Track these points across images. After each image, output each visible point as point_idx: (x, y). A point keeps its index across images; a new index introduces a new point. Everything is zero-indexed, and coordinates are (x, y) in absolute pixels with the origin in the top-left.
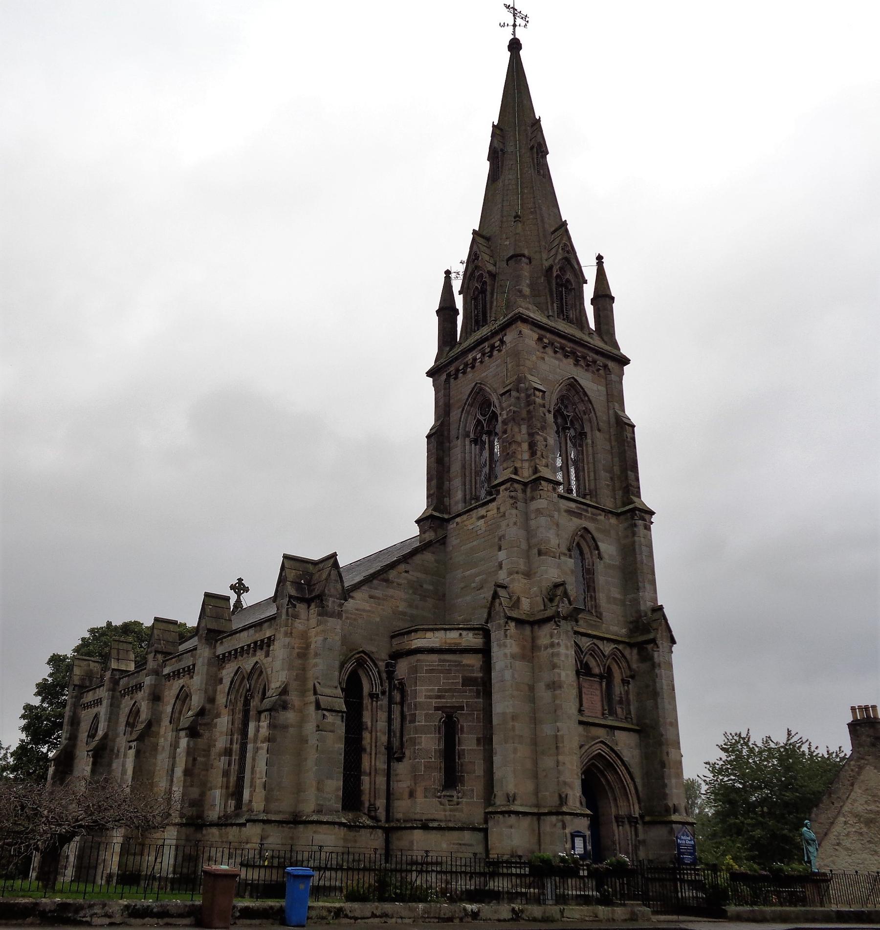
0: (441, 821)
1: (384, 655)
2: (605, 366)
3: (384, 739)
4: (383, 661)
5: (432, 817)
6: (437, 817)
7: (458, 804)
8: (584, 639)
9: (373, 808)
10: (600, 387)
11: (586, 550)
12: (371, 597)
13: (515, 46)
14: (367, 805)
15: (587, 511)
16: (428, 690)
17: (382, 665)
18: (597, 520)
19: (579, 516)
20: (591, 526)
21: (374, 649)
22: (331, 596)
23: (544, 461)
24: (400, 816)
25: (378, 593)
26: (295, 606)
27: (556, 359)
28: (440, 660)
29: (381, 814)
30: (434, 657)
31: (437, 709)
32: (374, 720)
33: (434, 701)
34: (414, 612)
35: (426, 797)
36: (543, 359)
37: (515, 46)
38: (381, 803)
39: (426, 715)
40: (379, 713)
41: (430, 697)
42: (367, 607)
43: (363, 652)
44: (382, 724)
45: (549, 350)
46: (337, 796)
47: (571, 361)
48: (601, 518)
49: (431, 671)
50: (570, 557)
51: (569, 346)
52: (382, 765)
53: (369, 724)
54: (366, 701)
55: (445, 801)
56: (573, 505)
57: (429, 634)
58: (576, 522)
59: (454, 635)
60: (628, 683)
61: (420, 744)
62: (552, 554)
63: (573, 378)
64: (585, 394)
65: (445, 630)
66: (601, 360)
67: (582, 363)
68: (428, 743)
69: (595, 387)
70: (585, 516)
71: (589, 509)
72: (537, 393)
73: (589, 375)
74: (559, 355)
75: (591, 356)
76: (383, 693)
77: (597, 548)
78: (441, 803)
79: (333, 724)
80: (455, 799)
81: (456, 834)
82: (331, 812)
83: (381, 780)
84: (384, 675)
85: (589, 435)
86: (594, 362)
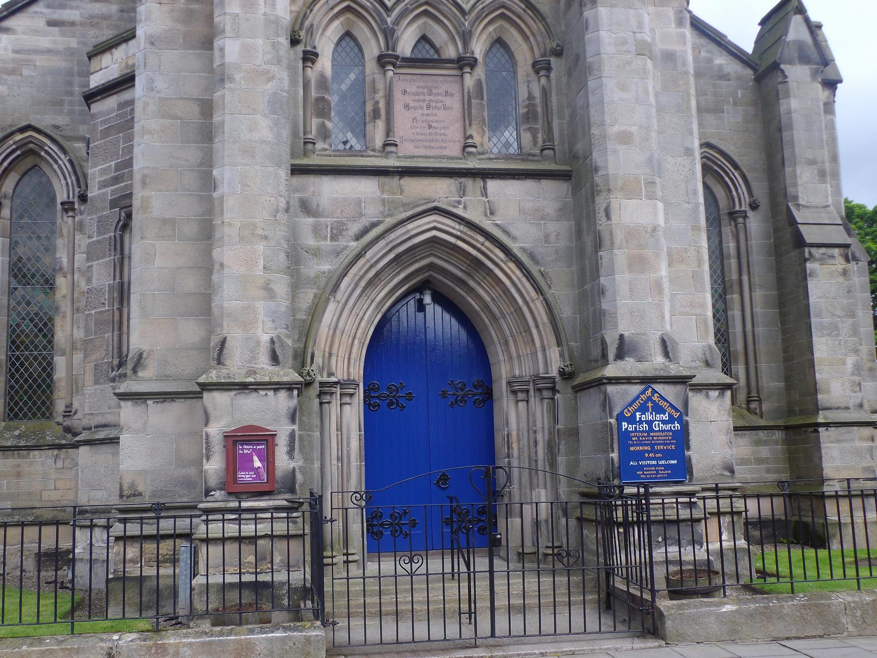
12: (51, 23)
14: (60, 407)
16: (104, 172)
33: (109, 189)
35: (96, 382)
42: (44, 42)
43: (29, 127)
49: (106, 133)
53: (65, 261)
60: (549, 69)
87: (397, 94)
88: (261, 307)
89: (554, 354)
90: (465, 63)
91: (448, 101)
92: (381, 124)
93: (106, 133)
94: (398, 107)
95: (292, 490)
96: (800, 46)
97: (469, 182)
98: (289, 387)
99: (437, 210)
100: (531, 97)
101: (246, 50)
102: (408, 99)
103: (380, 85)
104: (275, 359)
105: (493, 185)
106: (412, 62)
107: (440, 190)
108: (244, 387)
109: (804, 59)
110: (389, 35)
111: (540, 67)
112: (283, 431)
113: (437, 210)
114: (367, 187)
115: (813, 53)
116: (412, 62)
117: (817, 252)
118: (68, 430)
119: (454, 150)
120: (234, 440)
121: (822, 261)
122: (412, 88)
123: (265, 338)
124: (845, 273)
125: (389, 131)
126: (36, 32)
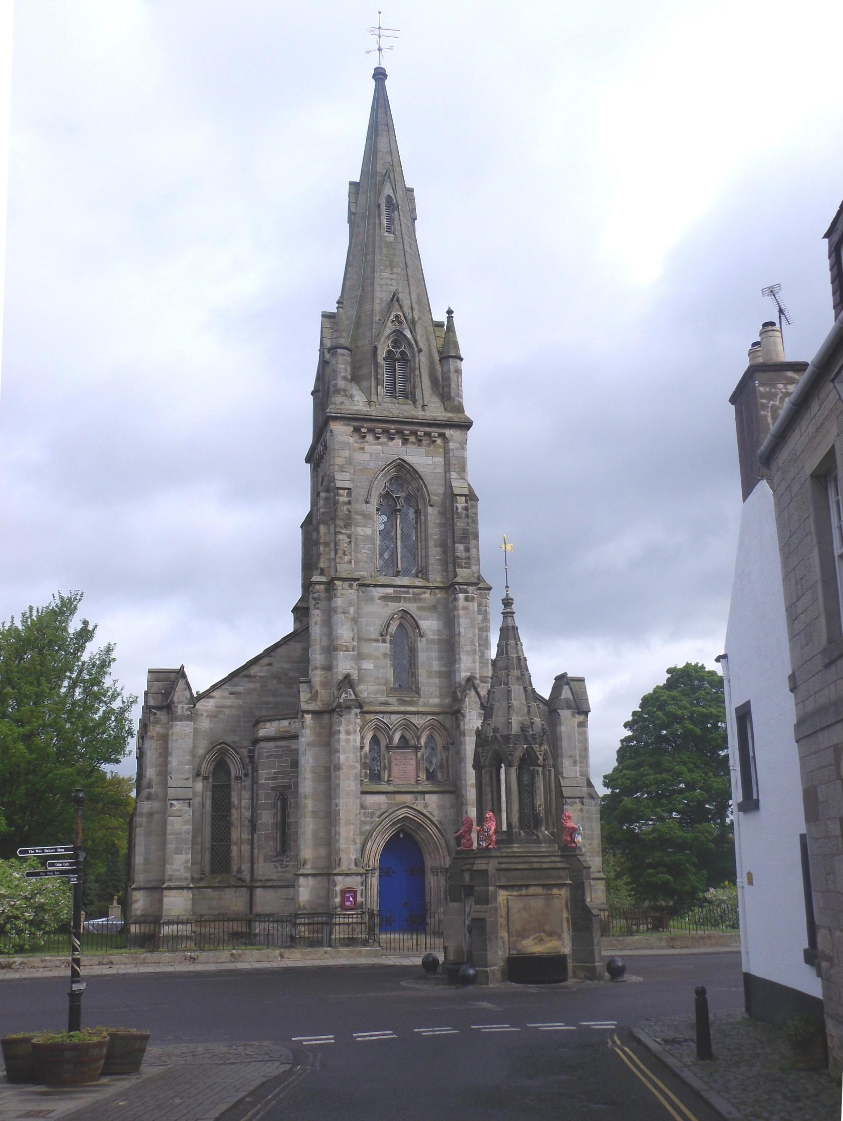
0: (275, 880)
1: (246, 743)
2: (442, 435)
3: (247, 814)
4: (246, 747)
5: (267, 877)
6: (273, 877)
7: (287, 866)
8: (394, 717)
9: (239, 871)
10: (435, 459)
11: (409, 629)
12: (231, 693)
13: (380, 75)
14: (235, 868)
15: (407, 593)
16: (267, 773)
17: (245, 752)
18: (420, 600)
19: (397, 599)
20: (412, 607)
21: (236, 739)
22: (179, 703)
23: (346, 558)
24: (260, 878)
25: (239, 689)
26: (155, 714)
27: (380, 444)
28: (277, 747)
29: (246, 875)
30: (271, 744)
31: (273, 788)
32: (240, 800)
34: (279, 700)
35: (265, 862)
36: (363, 449)
37: (380, 75)
38: (246, 867)
39: (266, 794)
40: (243, 792)
41: (267, 779)
42: (228, 702)
44: (245, 802)
45: (370, 438)
46: (186, 868)
47: (398, 441)
48: (427, 595)
49: (269, 757)
50: (384, 641)
51: (393, 428)
52: (246, 836)
53: (236, 802)
54: (234, 783)
55: (278, 864)
56: (390, 591)
57: (268, 725)
58: (394, 607)
59: (285, 723)
60: (448, 749)
61: (261, 819)
62: (344, 649)
63: (400, 459)
64: (416, 472)
65: (279, 720)
66: (435, 432)
67: (412, 439)
68: (267, 818)
69: (429, 460)
70: (405, 598)
71: (411, 590)
72: (341, 492)
73: (422, 450)
74: (383, 439)
75: (421, 430)
76: (246, 775)
77: (418, 627)
78: (275, 867)
79: (181, 810)
80: (284, 863)
81: (285, 890)
82: (181, 879)
83: (246, 848)
84: (247, 760)
85: (423, 512)
86: (428, 434)
87: (393, 760)
88: (352, 847)
89: (447, 859)
90: (417, 748)
91: (411, 762)
92: (386, 772)
93: (269, 757)
94: (393, 765)
95: (362, 908)
96: (567, 700)
97: (419, 796)
98: (361, 875)
99: (407, 807)
100: (442, 759)
101: (347, 758)
102: (397, 762)
103: (386, 756)
104: (356, 865)
105: (427, 796)
106: (397, 747)
107: (408, 798)
108: (347, 875)
109: (569, 707)
110: (391, 738)
111: (446, 749)
112: (359, 889)
113: (407, 807)
114: (382, 798)
115: (574, 705)
116: (397, 747)
117: (569, 801)
118: (239, 879)
119: (413, 781)
120: (343, 892)
121: (571, 804)
122: (398, 757)
123: (353, 858)
124: (581, 810)
125: (389, 776)
126: (224, 698)
